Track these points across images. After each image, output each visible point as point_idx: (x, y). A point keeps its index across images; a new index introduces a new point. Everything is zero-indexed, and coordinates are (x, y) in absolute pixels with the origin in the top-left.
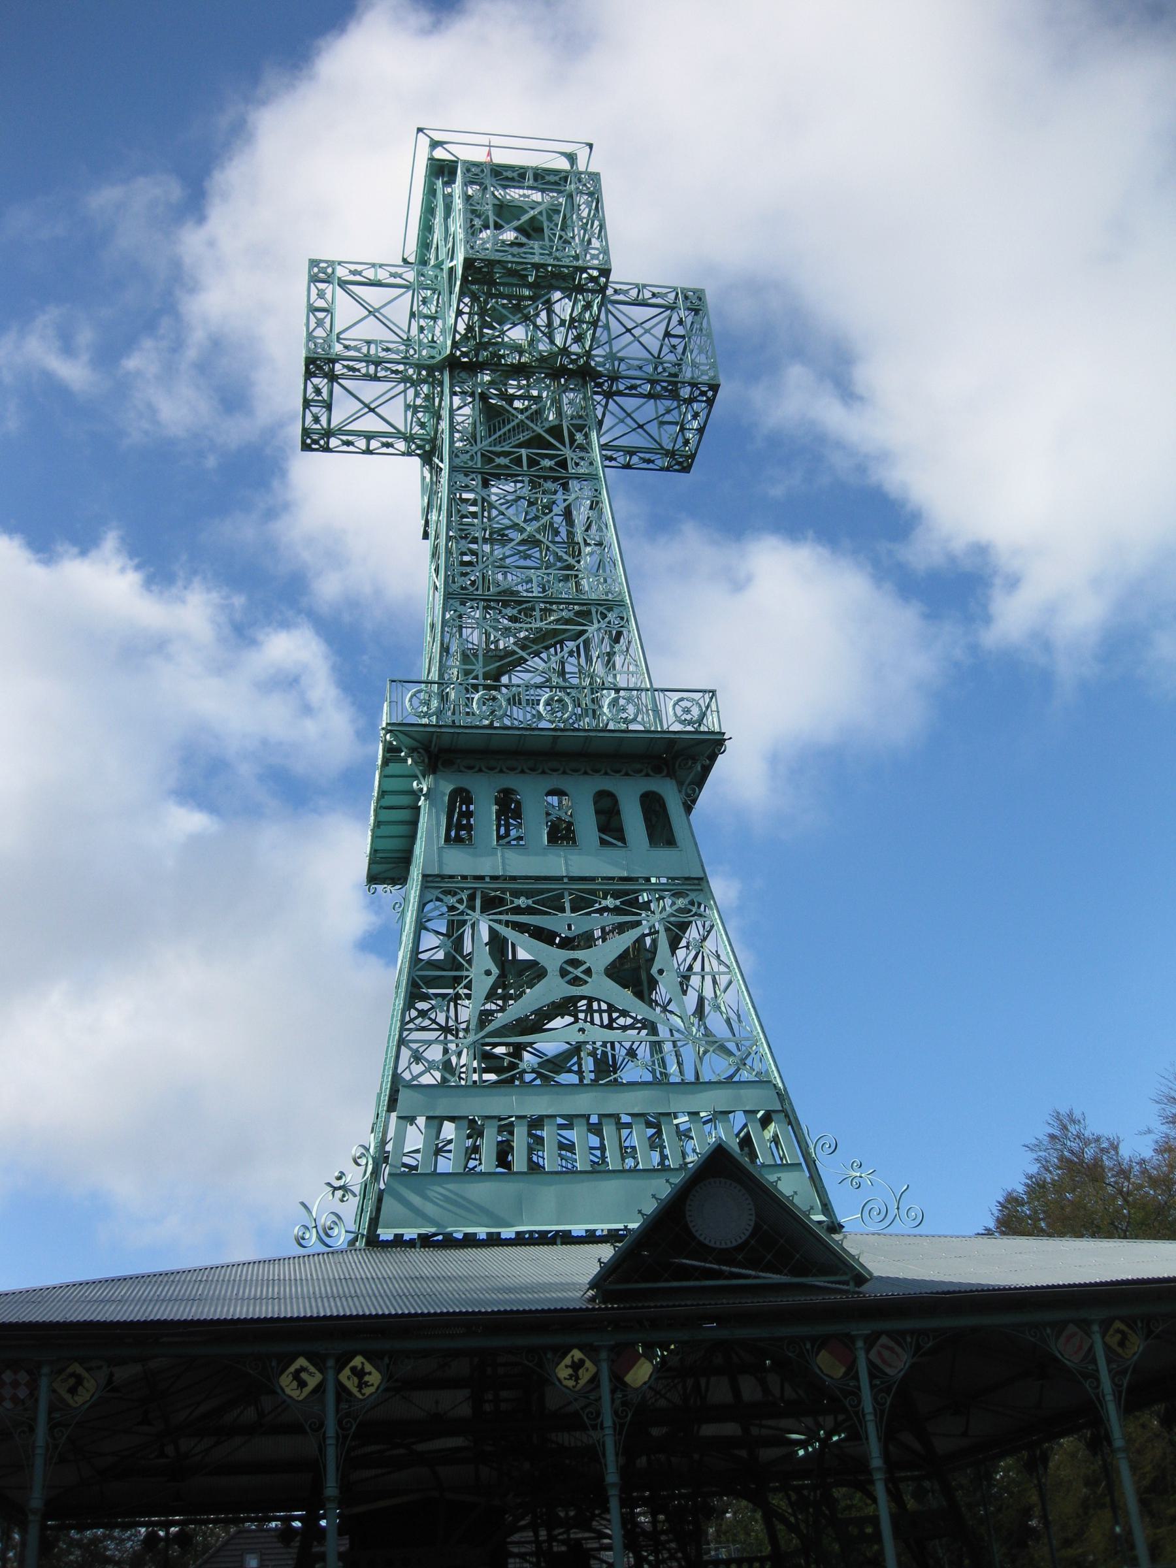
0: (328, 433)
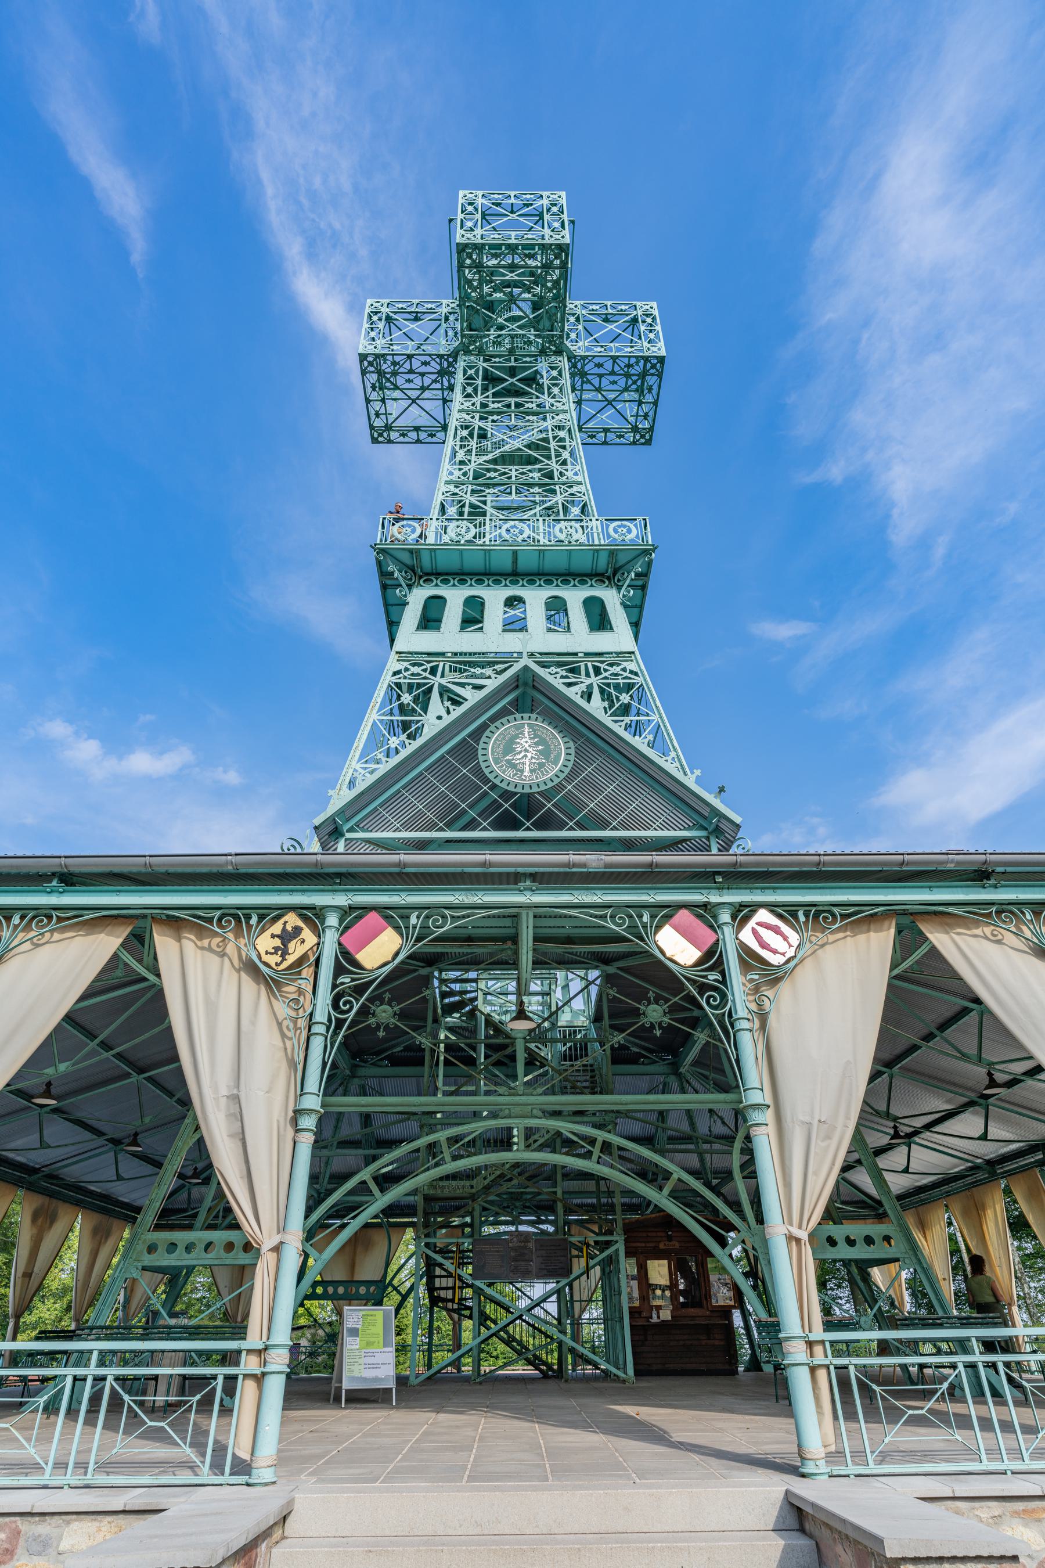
0: (388, 428)
